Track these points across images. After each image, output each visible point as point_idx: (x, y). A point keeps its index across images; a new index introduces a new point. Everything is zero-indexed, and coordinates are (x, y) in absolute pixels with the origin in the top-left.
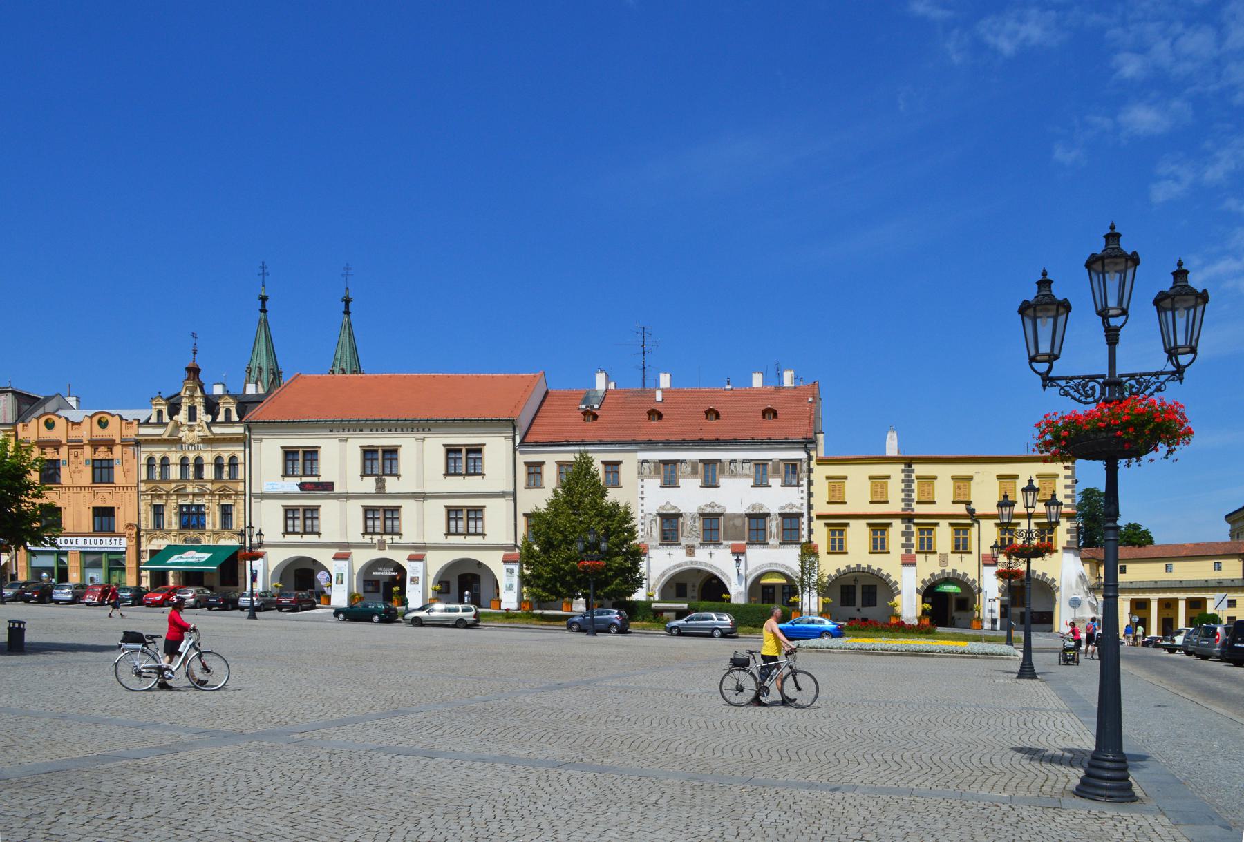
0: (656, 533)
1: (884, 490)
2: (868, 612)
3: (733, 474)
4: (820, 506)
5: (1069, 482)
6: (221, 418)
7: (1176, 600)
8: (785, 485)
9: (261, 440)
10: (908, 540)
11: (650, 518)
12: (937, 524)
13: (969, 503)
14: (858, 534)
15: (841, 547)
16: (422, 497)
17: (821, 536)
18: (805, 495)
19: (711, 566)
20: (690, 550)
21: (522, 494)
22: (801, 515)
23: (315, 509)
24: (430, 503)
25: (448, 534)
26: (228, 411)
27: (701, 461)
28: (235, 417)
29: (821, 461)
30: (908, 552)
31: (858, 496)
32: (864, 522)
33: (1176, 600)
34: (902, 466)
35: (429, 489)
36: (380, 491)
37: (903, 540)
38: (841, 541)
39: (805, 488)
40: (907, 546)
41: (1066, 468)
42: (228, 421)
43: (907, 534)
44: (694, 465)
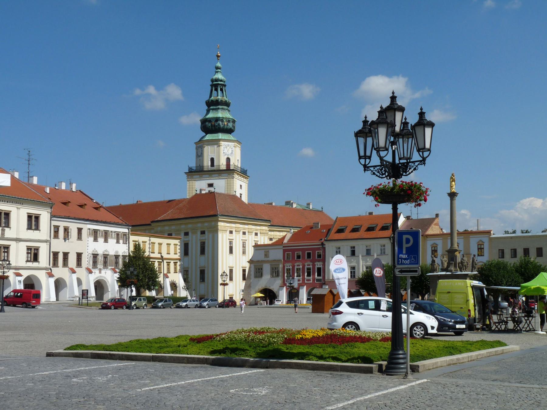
11: (90, 255)
13: (161, 253)
16: (18, 240)
20: (100, 270)
24: (21, 243)
35: (22, 237)
39: (128, 245)
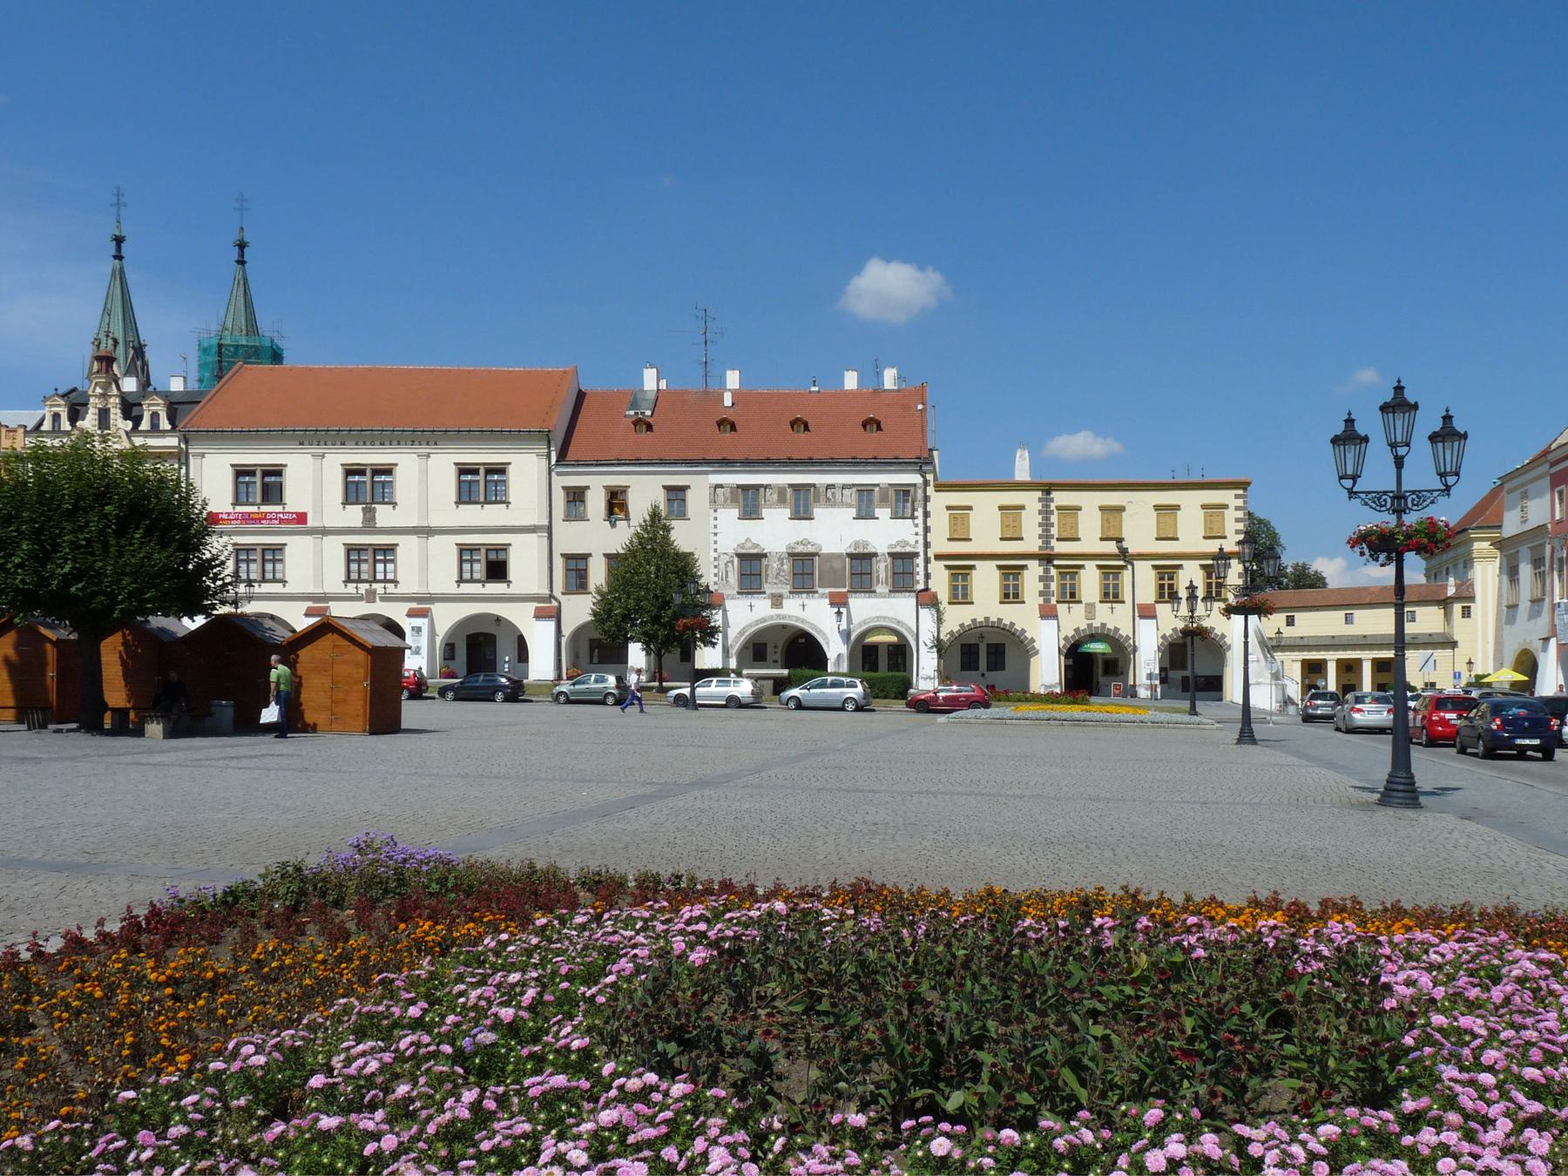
0: (733, 578)
1: (1017, 524)
2: (995, 677)
3: (830, 503)
4: (940, 544)
5: (1240, 514)
6: (145, 425)
7: (1359, 662)
8: (895, 517)
9: (203, 455)
10: (1047, 586)
11: (725, 559)
12: (1082, 567)
13: (1119, 540)
14: (986, 579)
15: (965, 595)
16: (427, 532)
17: (940, 582)
18: (920, 530)
19: (803, 621)
20: (777, 601)
21: (560, 527)
22: (916, 555)
23: (280, 548)
25: (461, 580)
26: (155, 416)
27: (790, 485)
28: (165, 424)
29: (940, 487)
30: (1047, 601)
31: (985, 533)
32: (992, 565)
33: (1359, 662)
34: (1039, 494)
35: (435, 522)
36: (369, 525)
37: (1041, 586)
38: (965, 588)
39: (920, 521)
40: (1045, 593)
41: (1237, 497)
42: (155, 429)
43: (1045, 579)
44: (781, 491)
